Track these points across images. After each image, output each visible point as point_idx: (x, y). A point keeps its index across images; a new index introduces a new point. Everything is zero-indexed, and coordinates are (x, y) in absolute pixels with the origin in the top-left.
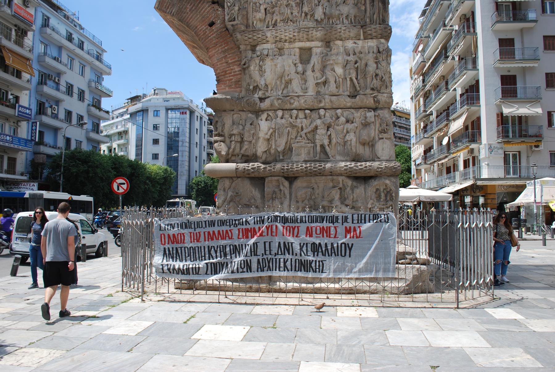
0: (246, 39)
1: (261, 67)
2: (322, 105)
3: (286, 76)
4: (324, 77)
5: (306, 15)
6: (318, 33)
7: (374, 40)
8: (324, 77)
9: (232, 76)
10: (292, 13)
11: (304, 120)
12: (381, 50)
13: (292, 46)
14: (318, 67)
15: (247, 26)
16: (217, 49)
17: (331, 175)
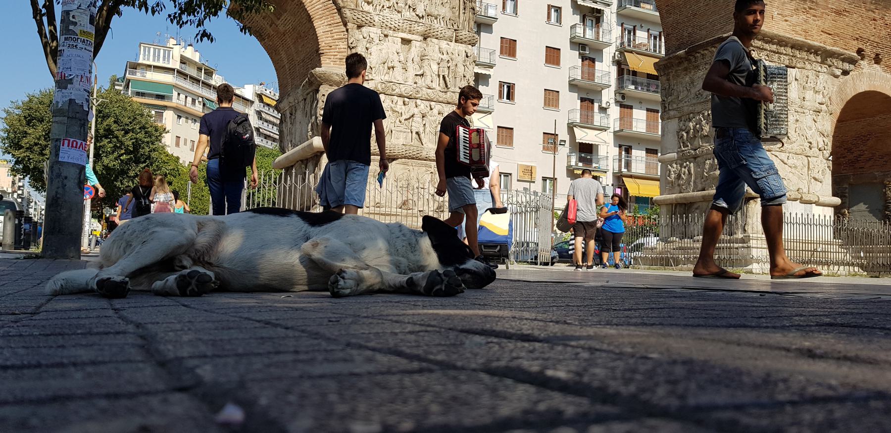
0: (355, 18)
1: (367, 49)
2: (419, 95)
3: (390, 63)
4: (422, 71)
5: (410, 7)
6: (418, 28)
7: (464, 45)
8: (422, 71)
9: (337, 52)
10: (397, 3)
11: (403, 107)
12: (469, 55)
13: (395, 35)
14: (417, 59)
15: (357, 5)
16: (323, 21)
17: (425, 160)
